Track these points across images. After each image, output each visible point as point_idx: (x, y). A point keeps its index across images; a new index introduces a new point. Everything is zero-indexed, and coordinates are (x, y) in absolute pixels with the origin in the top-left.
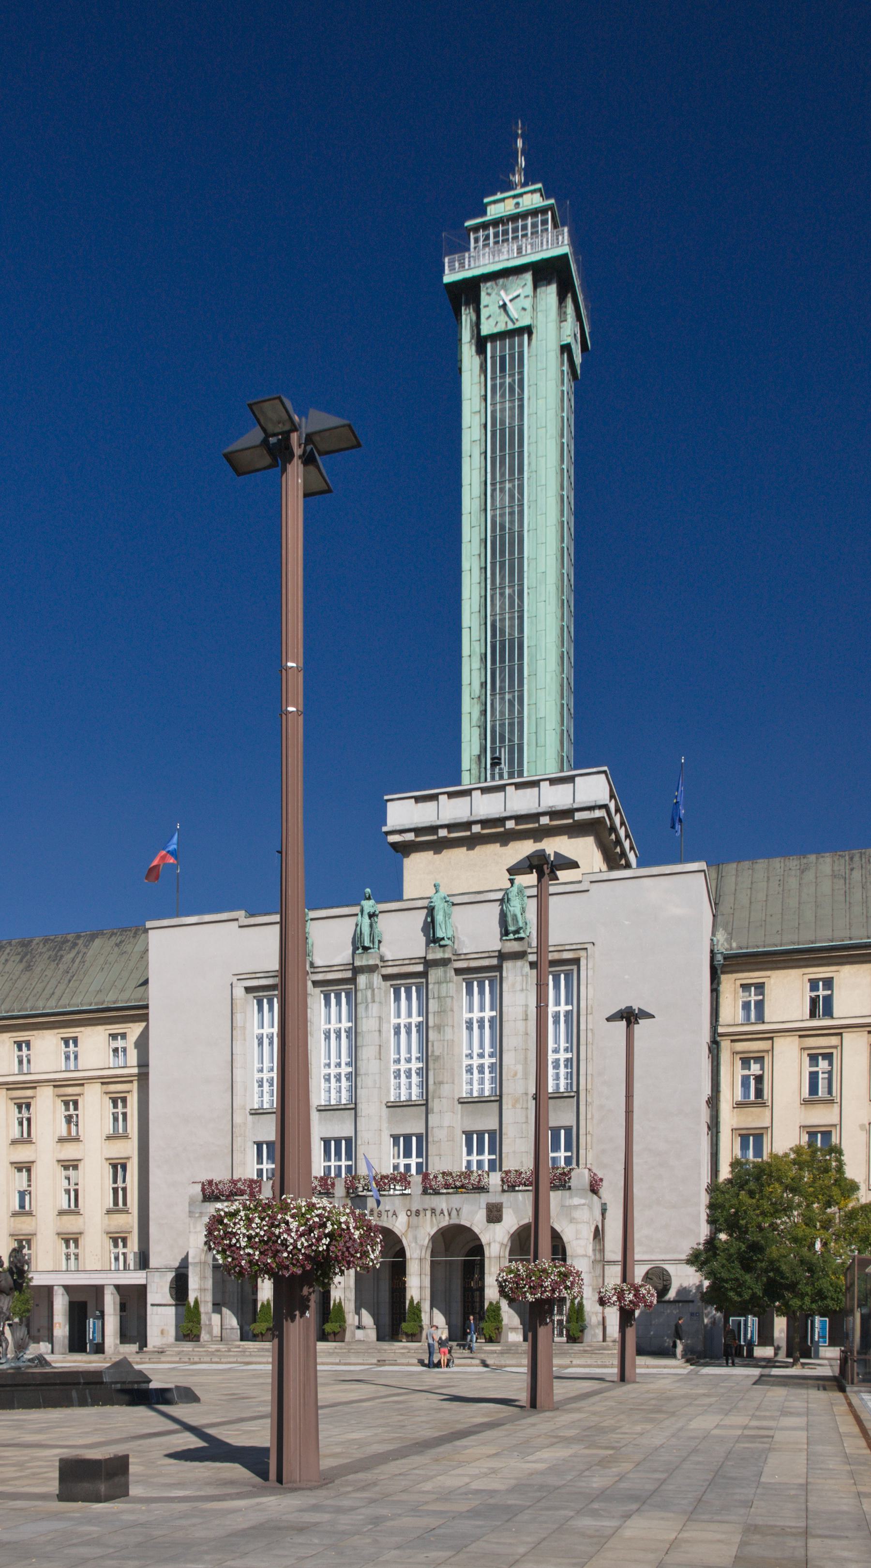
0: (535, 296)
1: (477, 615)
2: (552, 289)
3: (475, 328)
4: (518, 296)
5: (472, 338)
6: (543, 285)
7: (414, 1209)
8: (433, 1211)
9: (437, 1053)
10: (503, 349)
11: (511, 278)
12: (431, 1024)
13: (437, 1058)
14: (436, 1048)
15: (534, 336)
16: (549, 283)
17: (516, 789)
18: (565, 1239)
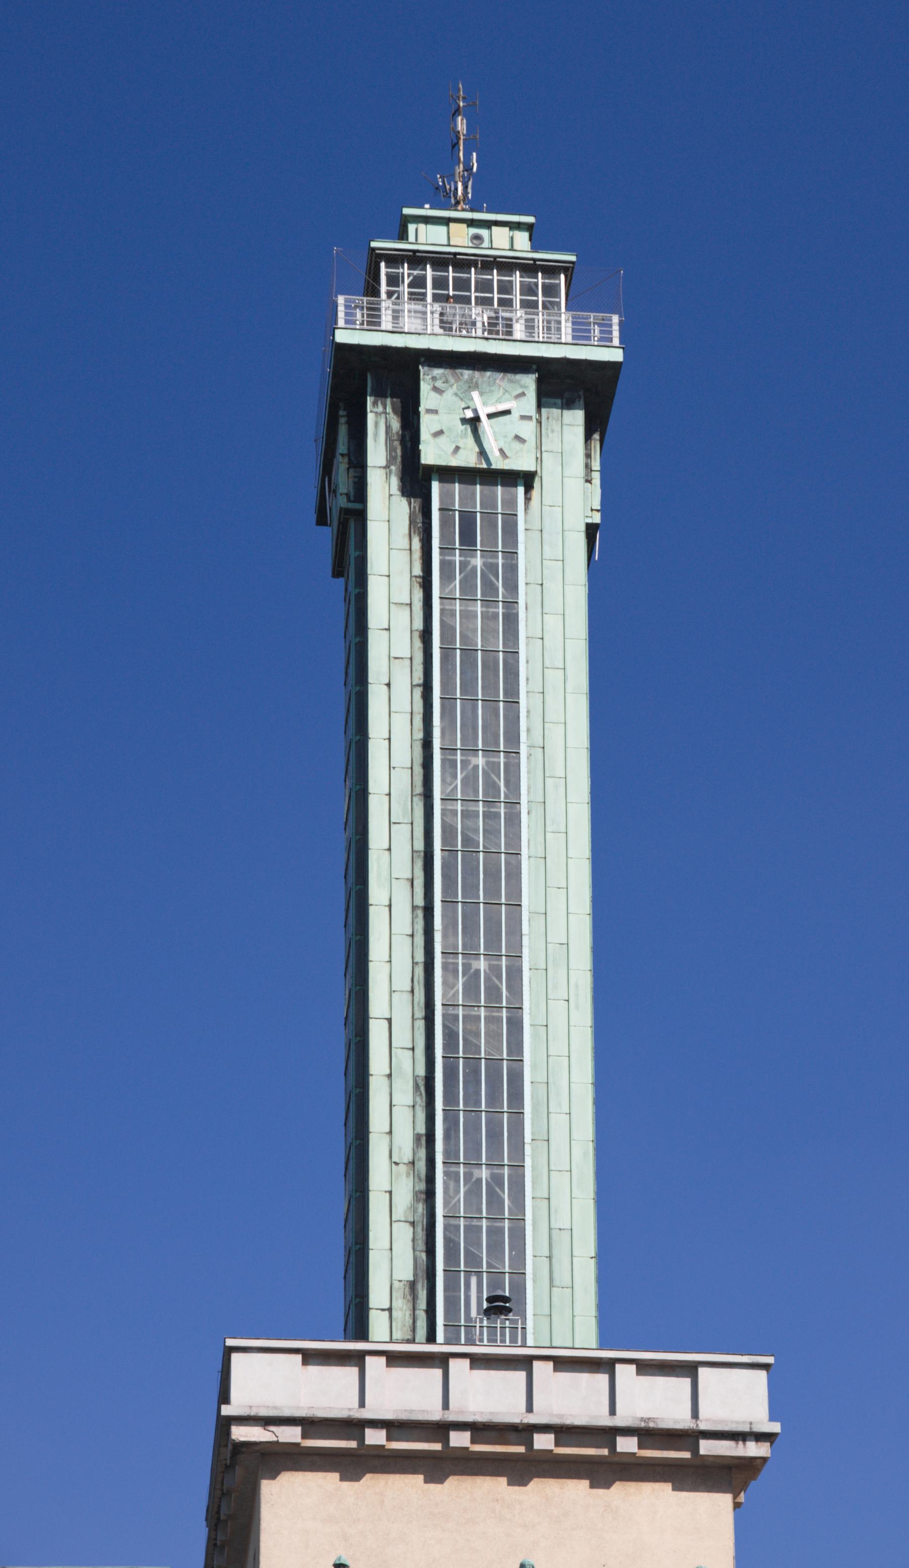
0: (539, 422)
1: (409, 996)
2: (576, 418)
3: (397, 444)
4: (507, 412)
5: (390, 461)
6: (555, 406)
10: (468, 498)
11: (488, 374)
15: (535, 493)
16: (568, 405)
17: (556, 1369)
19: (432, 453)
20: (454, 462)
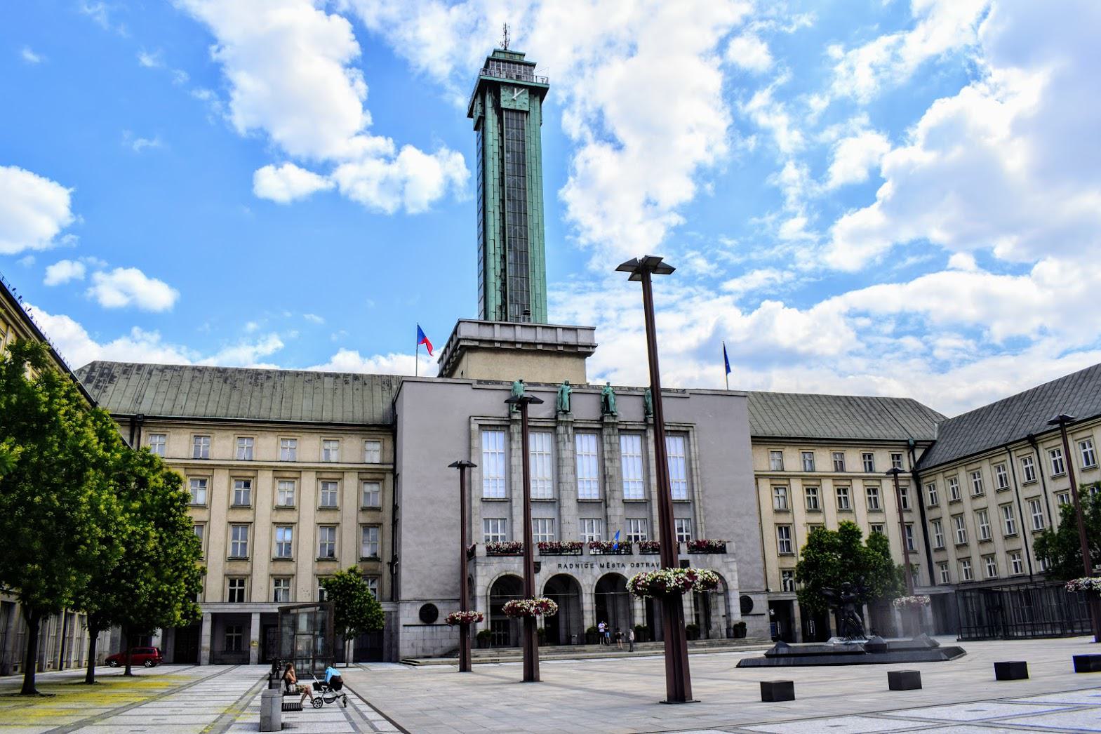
5: (493, 106)
7: (635, 564)
8: (648, 564)
9: (610, 474)
12: (606, 457)
13: (611, 477)
14: (611, 471)
18: (727, 581)
19: (504, 105)
20: (509, 107)
